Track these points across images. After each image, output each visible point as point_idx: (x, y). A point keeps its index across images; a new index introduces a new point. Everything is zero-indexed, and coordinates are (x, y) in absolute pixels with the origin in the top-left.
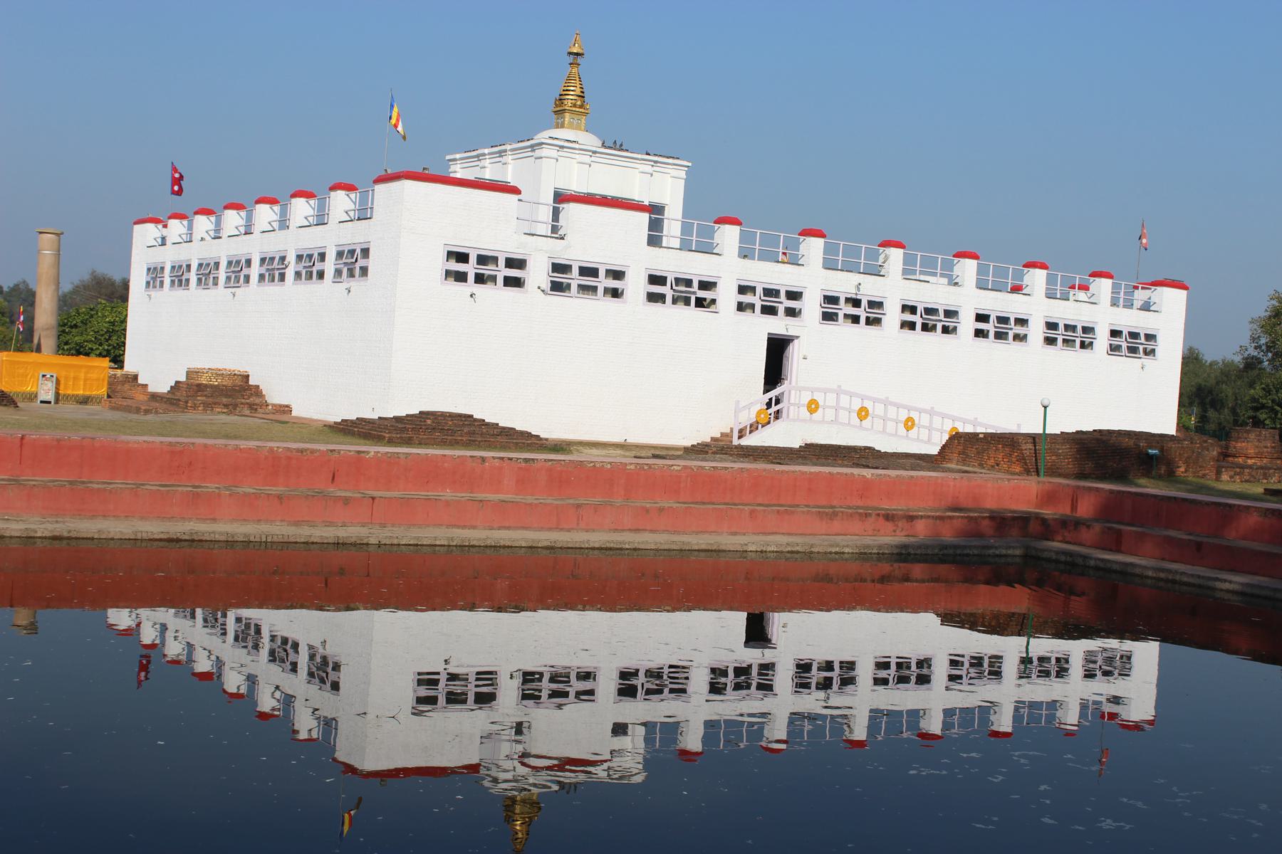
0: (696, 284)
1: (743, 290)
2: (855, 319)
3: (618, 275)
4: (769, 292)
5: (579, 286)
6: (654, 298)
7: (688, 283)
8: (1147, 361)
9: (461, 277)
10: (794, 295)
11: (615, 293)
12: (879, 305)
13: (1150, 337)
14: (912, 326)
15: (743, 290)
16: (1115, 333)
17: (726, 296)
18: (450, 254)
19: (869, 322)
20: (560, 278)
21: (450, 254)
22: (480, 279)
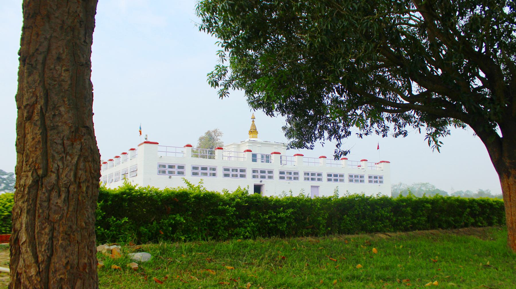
0: (239, 170)
1: (254, 171)
2: (290, 178)
3: (214, 169)
4: (262, 172)
5: (202, 173)
6: (226, 175)
7: (237, 170)
8: (381, 184)
9: (164, 172)
10: (270, 172)
11: (214, 175)
12: (297, 173)
13: (381, 178)
14: (308, 179)
15: (254, 171)
16: (370, 177)
17: (249, 174)
18: (160, 166)
19: (295, 179)
20: (195, 171)
21: (160, 166)
22: (171, 172)
